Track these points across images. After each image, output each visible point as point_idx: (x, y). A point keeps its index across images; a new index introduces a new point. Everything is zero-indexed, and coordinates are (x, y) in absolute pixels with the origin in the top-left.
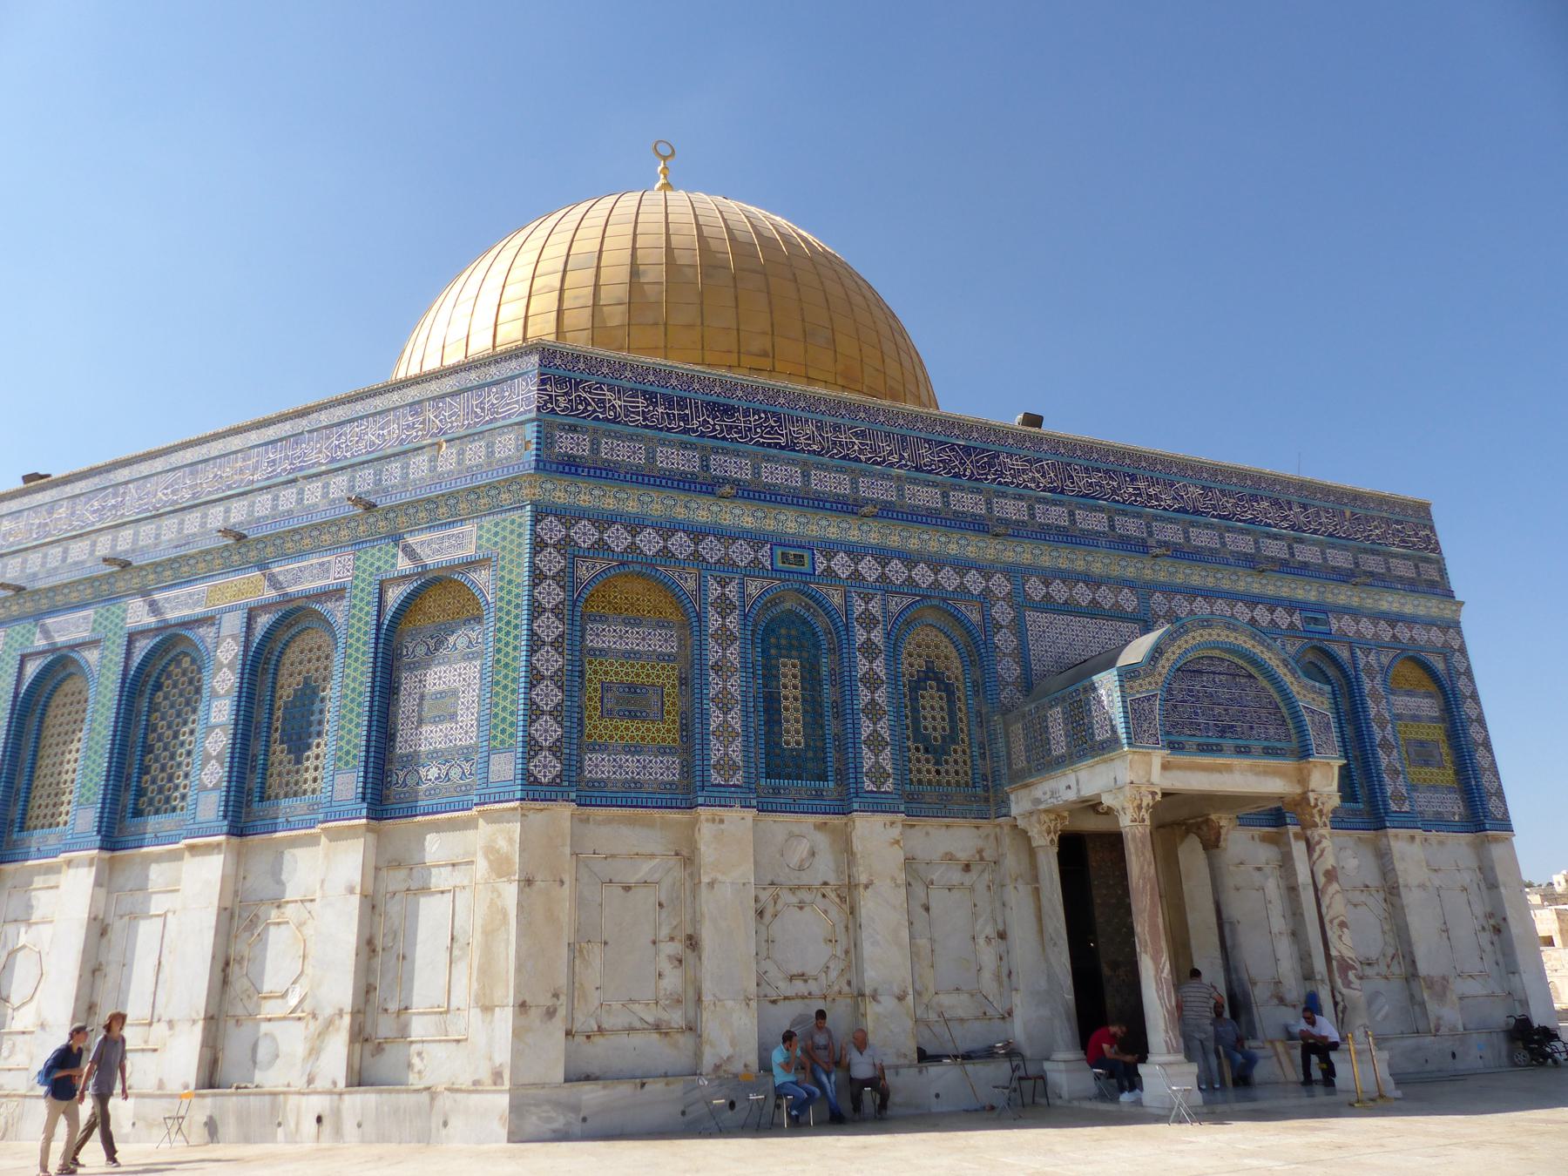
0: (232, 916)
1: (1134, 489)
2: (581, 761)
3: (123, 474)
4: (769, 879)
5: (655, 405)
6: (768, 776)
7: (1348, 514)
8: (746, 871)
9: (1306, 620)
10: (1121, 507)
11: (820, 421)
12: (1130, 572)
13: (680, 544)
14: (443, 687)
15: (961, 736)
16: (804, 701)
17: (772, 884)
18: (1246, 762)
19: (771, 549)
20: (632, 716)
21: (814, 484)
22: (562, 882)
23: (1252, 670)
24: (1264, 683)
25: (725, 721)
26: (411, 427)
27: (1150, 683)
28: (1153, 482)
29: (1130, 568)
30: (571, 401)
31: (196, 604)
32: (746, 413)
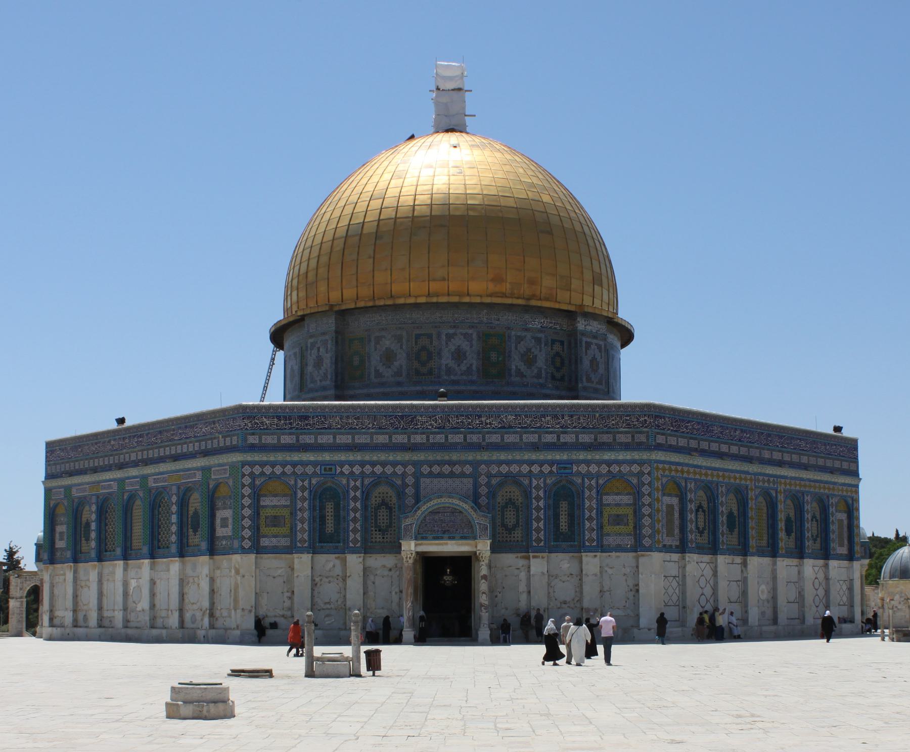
1: (479, 421)
4: (319, 574)
5: (280, 420)
6: (320, 542)
7: (597, 415)
8: (309, 572)
11: (342, 416)
12: (470, 458)
17: (320, 576)
18: (453, 542)
19: (320, 467)
20: (275, 526)
21: (338, 441)
22: (253, 576)
26: (213, 428)
29: (470, 456)
31: (165, 481)
32: (313, 418)
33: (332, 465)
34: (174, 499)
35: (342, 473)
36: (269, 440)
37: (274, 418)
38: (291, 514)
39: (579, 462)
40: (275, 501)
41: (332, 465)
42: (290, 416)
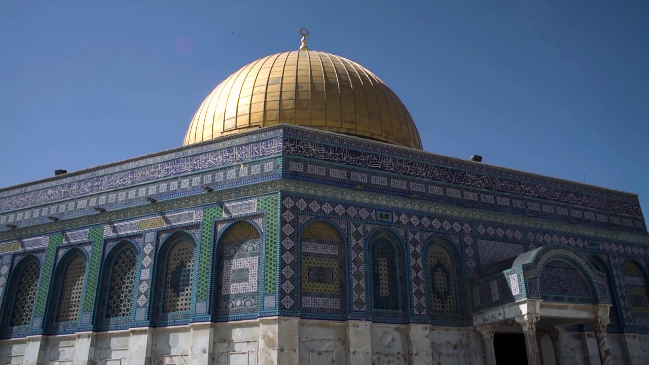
0: (150, 361)
2: (301, 299)
3: (101, 172)
5: (329, 151)
8: (367, 347)
9: (590, 244)
10: (515, 195)
11: (394, 158)
13: (339, 209)
14: (242, 267)
15: (452, 292)
16: (389, 276)
17: (377, 353)
18: (573, 305)
19: (376, 212)
20: (321, 281)
21: (392, 185)
22: (295, 350)
23: (574, 266)
24: (579, 272)
25: (358, 284)
26: (227, 158)
27: (535, 272)
28: (527, 185)
29: (519, 221)
30: (295, 149)
31: (135, 228)
32: (365, 155)
33: (387, 211)
34: (148, 249)
35: (399, 222)
36: (316, 170)
37: (321, 147)
38: (340, 268)
39: (603, 240)
40: (320, 249)
41: (387, 211)
42: (340, 148)
